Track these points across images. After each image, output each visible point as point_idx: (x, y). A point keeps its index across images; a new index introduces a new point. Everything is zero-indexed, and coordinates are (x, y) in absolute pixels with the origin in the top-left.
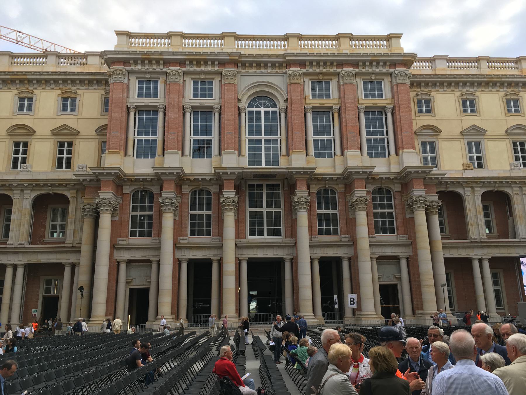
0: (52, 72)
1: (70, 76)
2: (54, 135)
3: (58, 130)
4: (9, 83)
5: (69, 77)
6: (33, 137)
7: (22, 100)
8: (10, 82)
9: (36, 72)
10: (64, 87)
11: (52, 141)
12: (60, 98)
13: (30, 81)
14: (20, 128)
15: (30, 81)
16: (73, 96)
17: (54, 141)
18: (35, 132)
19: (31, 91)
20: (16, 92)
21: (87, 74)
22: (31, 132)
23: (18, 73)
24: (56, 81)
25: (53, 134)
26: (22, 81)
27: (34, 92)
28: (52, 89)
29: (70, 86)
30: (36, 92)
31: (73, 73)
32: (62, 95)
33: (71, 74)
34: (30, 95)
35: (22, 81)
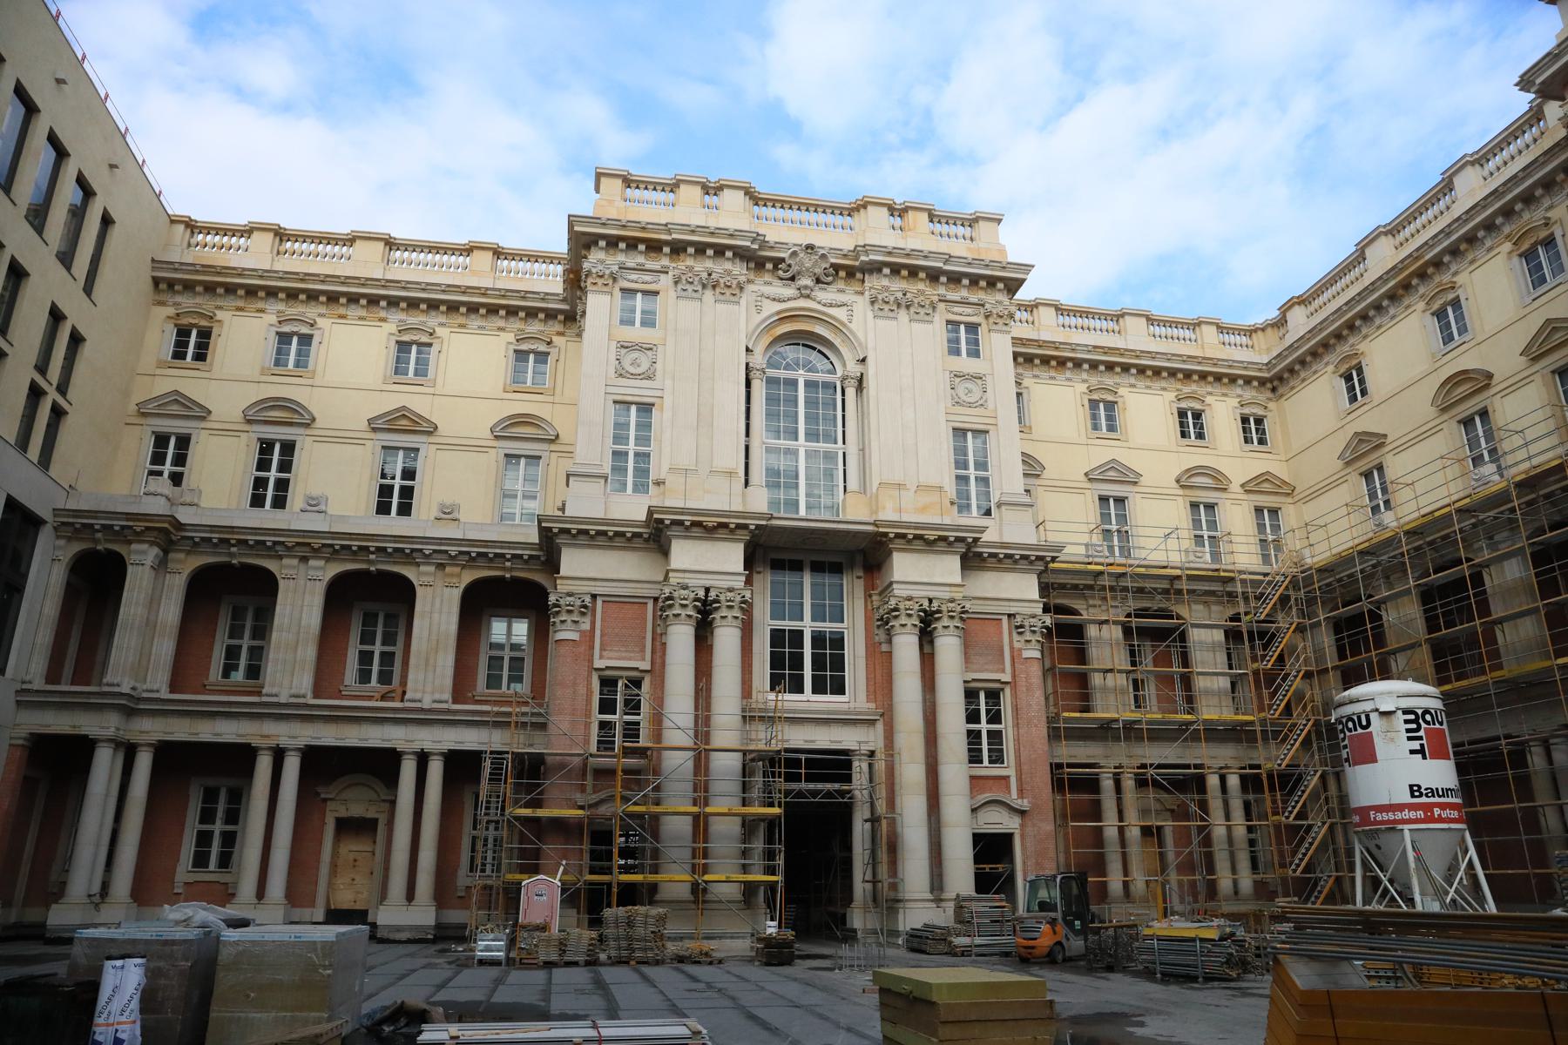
0: (1467, 212)
1: (1511, 191)
2: (1535, 359)
3: (1538, 344)
4: (1402, 296)
5: (1509, 197)
6: (1493, 391)
7: (1440, 315)
8: (1401, 292)
9: (1436, 236)
10: (1514, 227)
11: (1537, 377)
12: (1516, 260)
13: (1437, 263)
14: (1457, 384)
15: (1437, 263)
16: (1543, 234)
17: (1543, 376)
18: (1490, 376)
19: (1446, 284)
20: (1421, 305)
21: (1548, 156)
22: (1480, 381)
23: (1406, 263)
24: (1489, 226)
25: (1532, 359)
26: (1422, 275)
27: (1455, 283)
28: (1490, 249)
29: (1526, 216)
30: (1459, 279)
31: (1514, 180)
32: (1518, 249)
33: (1509, 185)
34: (1451, 296)
35: (1422, 275)
